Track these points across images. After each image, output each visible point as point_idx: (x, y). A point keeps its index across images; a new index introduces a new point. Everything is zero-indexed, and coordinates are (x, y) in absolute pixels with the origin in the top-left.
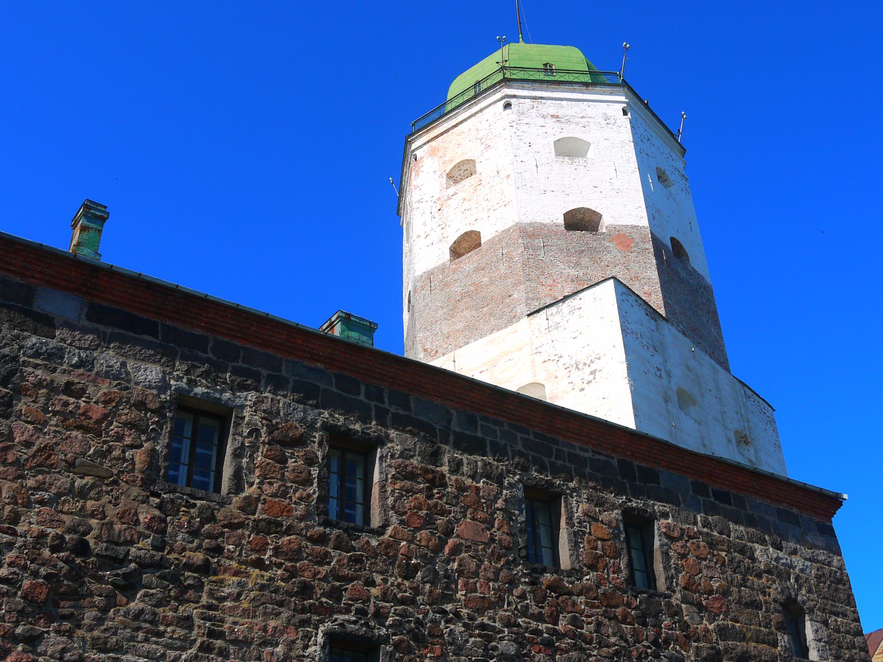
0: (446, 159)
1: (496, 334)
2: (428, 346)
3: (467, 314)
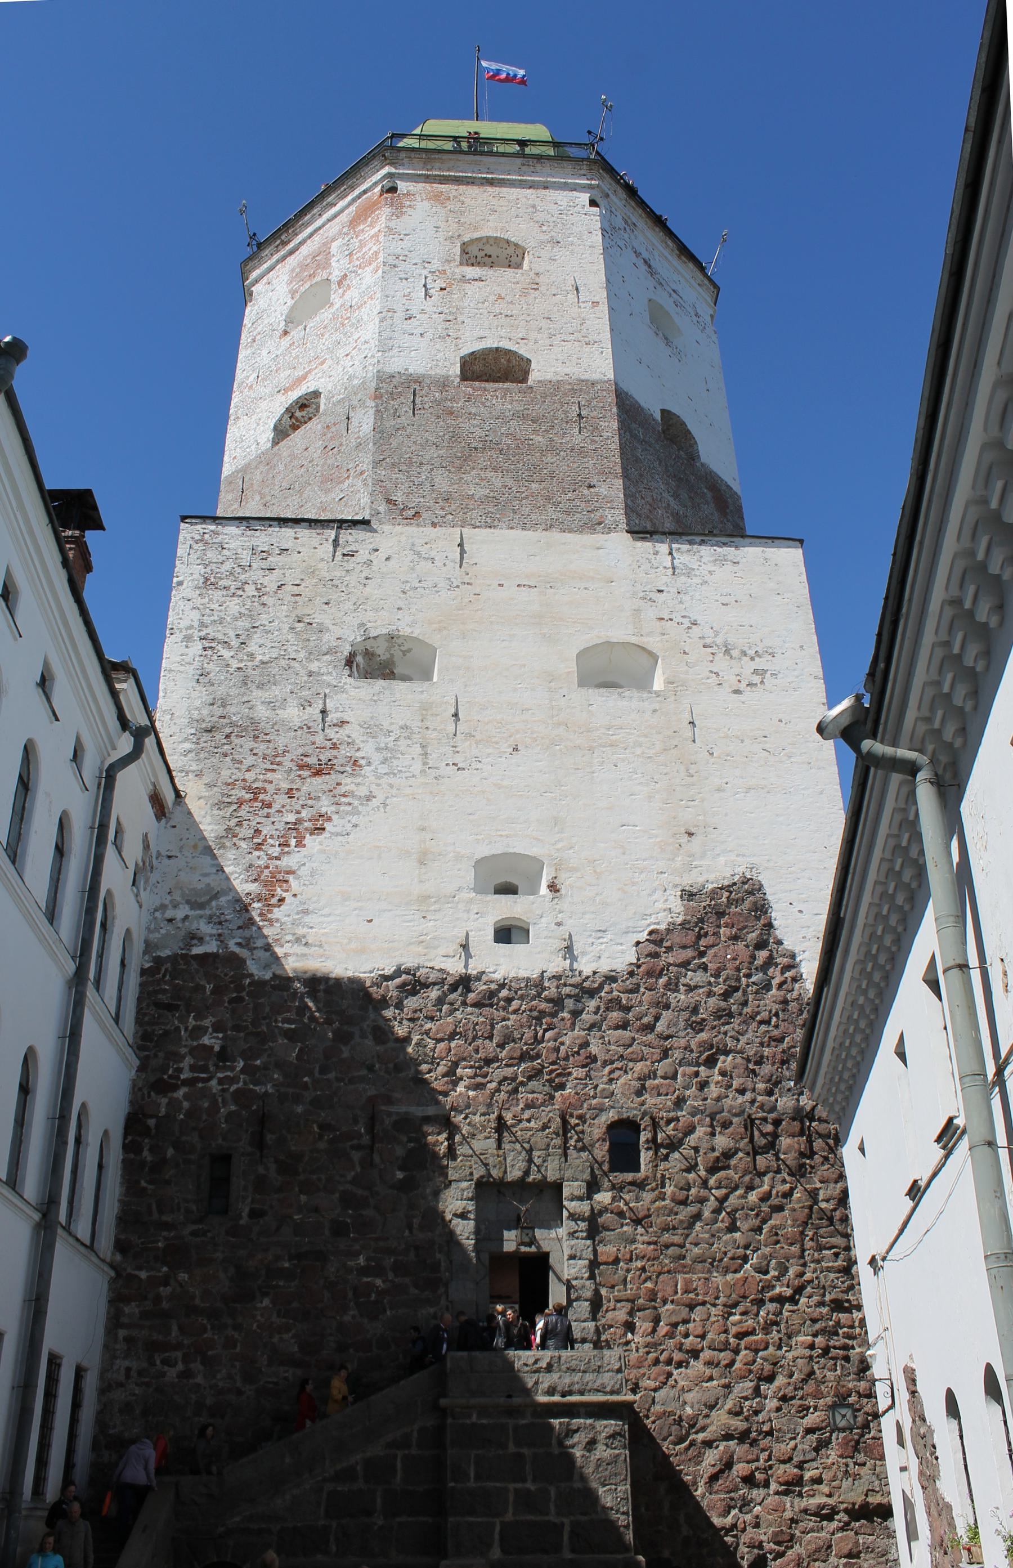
1: (555, 535)
2: (399, 497)
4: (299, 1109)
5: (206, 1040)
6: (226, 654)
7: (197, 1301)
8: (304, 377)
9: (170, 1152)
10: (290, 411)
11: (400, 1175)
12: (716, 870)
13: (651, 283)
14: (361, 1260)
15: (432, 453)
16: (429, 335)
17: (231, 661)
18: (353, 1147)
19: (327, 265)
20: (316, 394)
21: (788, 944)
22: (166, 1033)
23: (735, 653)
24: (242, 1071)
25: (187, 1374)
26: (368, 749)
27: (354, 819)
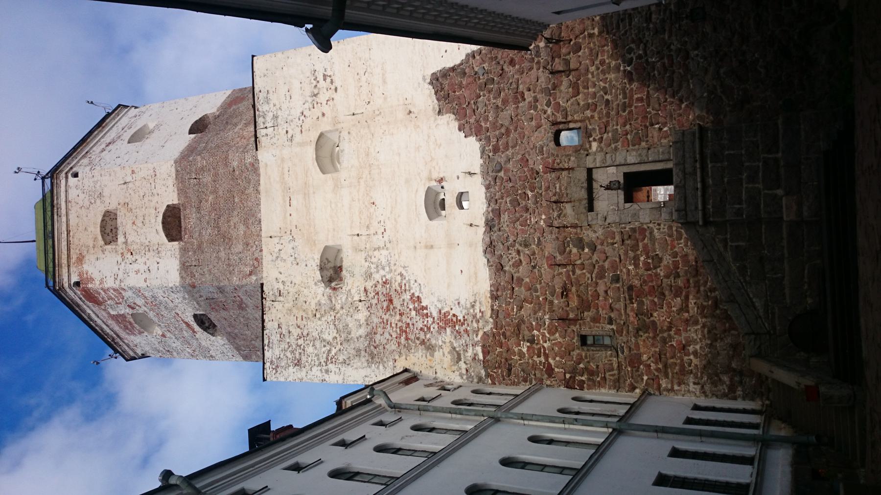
0: (91, 245)
1: (262, 188)
2: (247, 270)
3: (235, 219)
4: (556, 302)
5: (525, 350)
6: (334, 351)
7: (657, 350)
8: (186, 323)
9: (581, 366)
10: (206, 329)
11: (586, 250)
12: (426, 98)
13: (119, 142)
14: (631, 268)
15: (222, 254)
16: (158, 260)
17: (337, 349)
18: (574, 274)
19: (123, 316)
20: (195, 316)
21: (464, 57)
22: (523, 370)
23: (316, 92)
24: (539, 331)
25: (695, 353)
26: (377, 277)
27: (412, 282)
